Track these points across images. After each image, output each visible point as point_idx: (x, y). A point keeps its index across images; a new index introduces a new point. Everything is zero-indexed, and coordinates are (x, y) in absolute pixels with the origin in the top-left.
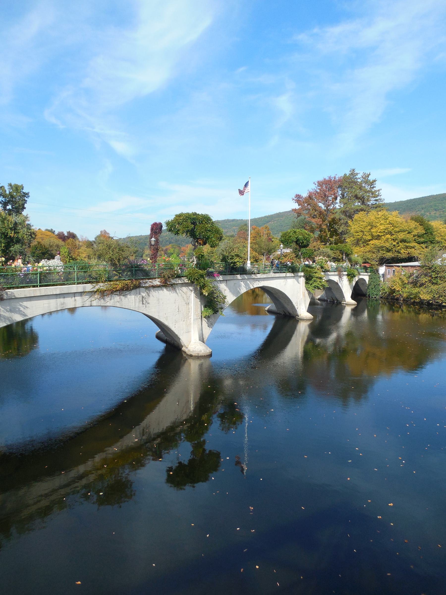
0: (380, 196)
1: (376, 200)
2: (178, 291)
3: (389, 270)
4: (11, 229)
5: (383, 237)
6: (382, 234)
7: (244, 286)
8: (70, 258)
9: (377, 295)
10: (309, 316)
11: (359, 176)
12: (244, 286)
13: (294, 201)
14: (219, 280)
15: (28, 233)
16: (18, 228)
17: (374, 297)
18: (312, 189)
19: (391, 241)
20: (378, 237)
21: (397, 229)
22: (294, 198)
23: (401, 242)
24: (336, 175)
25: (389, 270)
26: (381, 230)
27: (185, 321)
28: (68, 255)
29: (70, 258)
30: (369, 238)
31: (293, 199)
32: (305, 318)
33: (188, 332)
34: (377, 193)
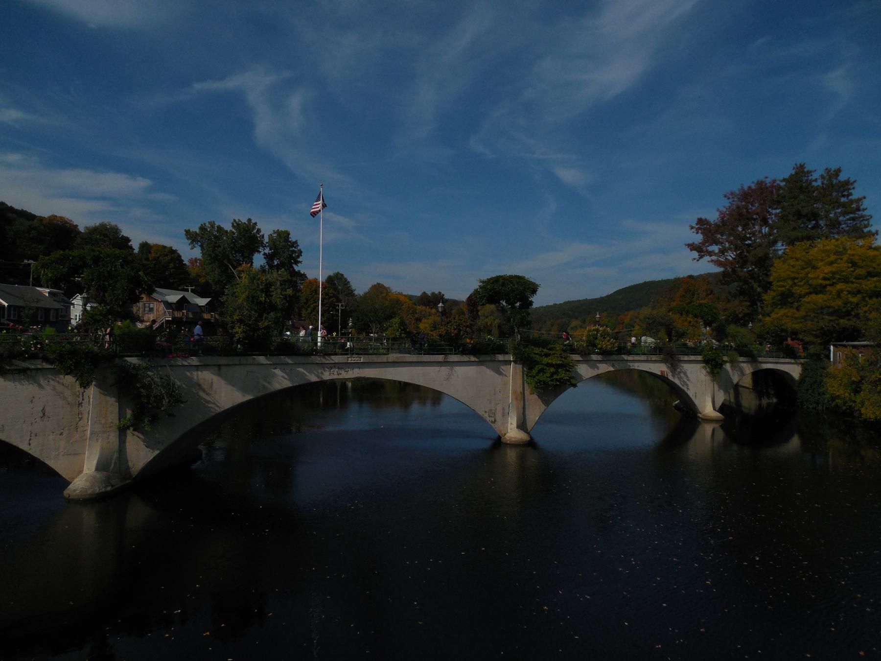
0: (864, 210)
1: (853, 219)
2: (42, 382)
3: (840, 354)
4: (262, 291)
5: (829, 288)
6: (828, 282)
7: (283, 377)
8: (402, 332)
9: (818, 403)
10: (515, 438)
11: (815, 176)
12: (283, 377)
13: (694, 230)
14: (181, 364)
15: (281, 296)
16: (271, 289)
17: (811, 407)
18: (725, 207)
19: (847, 295)
20: (819, 290)
21: (859, 271)
22: (694, 225)
23: (871, 297)
24: (766, 178)
25: (840, 354)
26: (826, 274)
27: (65, 434)
28: (399, 328)
29: (402, 332)
30: (804, 290)
31: (692, 228)
32: (508, 442)
33: (75, 454)
34: (854, 206)
